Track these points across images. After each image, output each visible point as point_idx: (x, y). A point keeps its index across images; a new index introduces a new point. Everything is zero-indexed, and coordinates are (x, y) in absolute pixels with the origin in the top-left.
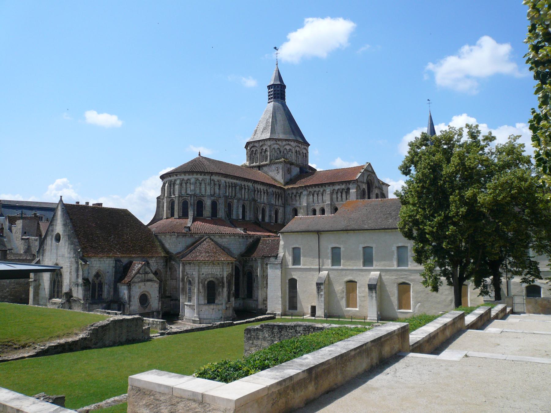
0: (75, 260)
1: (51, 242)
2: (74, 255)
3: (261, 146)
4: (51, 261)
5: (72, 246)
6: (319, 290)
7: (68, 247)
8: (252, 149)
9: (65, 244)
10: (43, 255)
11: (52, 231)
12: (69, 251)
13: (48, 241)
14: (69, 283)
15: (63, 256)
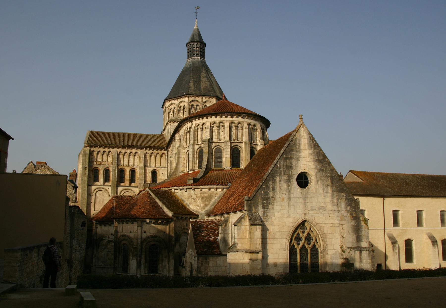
0: (351, 214)
1: (288, 185)
2: (346, 208)
3: (205, 102)
4: (289, 216)
5: (343, 194)
6: (394, 248)
7: (333, 195)
8: (192, 103)
9: (323, 190)
10: (265, 208)
11: (290, 167)
12: (336, 201)
13: (278, 185)
14: (340, 251)
15: (322, 209)
